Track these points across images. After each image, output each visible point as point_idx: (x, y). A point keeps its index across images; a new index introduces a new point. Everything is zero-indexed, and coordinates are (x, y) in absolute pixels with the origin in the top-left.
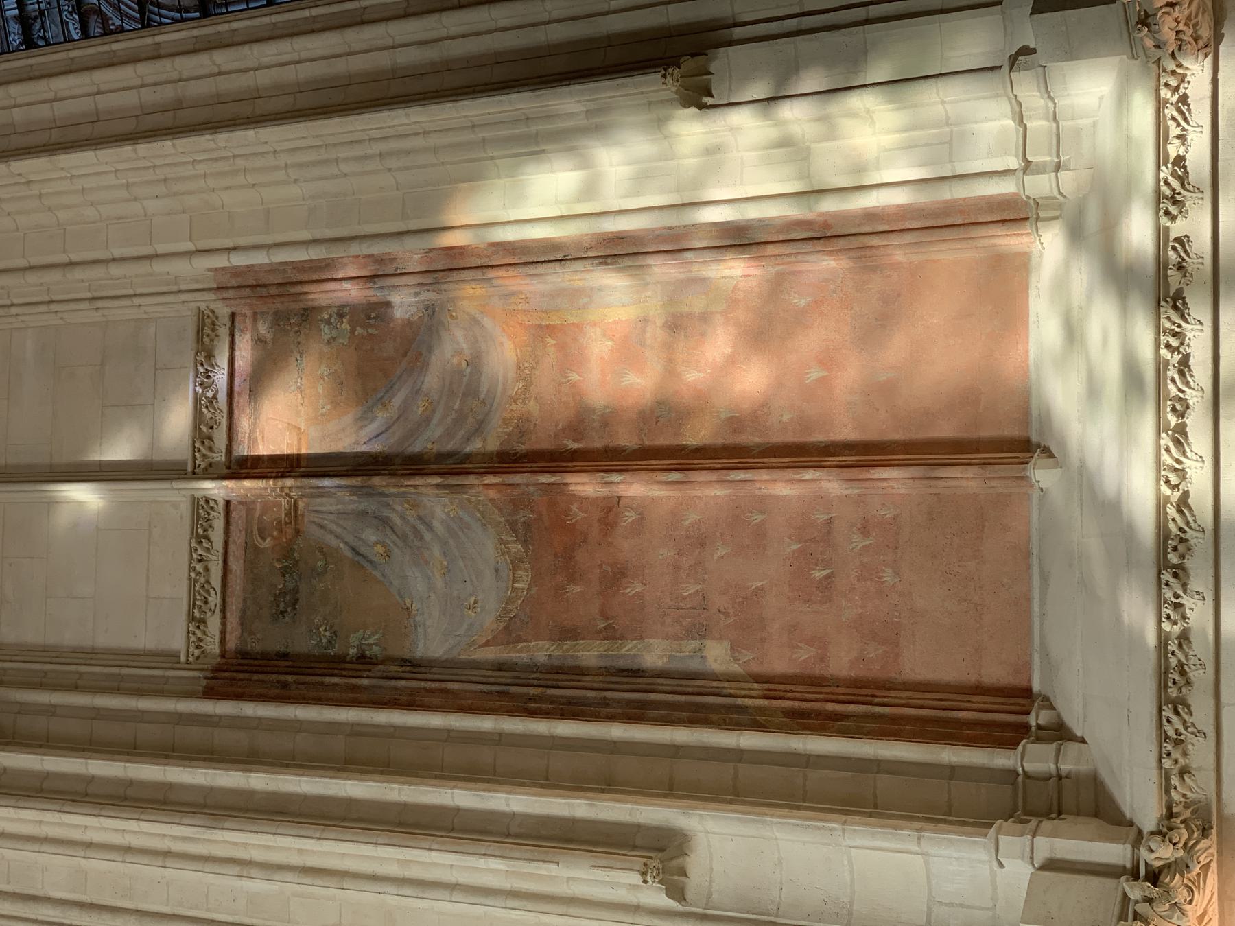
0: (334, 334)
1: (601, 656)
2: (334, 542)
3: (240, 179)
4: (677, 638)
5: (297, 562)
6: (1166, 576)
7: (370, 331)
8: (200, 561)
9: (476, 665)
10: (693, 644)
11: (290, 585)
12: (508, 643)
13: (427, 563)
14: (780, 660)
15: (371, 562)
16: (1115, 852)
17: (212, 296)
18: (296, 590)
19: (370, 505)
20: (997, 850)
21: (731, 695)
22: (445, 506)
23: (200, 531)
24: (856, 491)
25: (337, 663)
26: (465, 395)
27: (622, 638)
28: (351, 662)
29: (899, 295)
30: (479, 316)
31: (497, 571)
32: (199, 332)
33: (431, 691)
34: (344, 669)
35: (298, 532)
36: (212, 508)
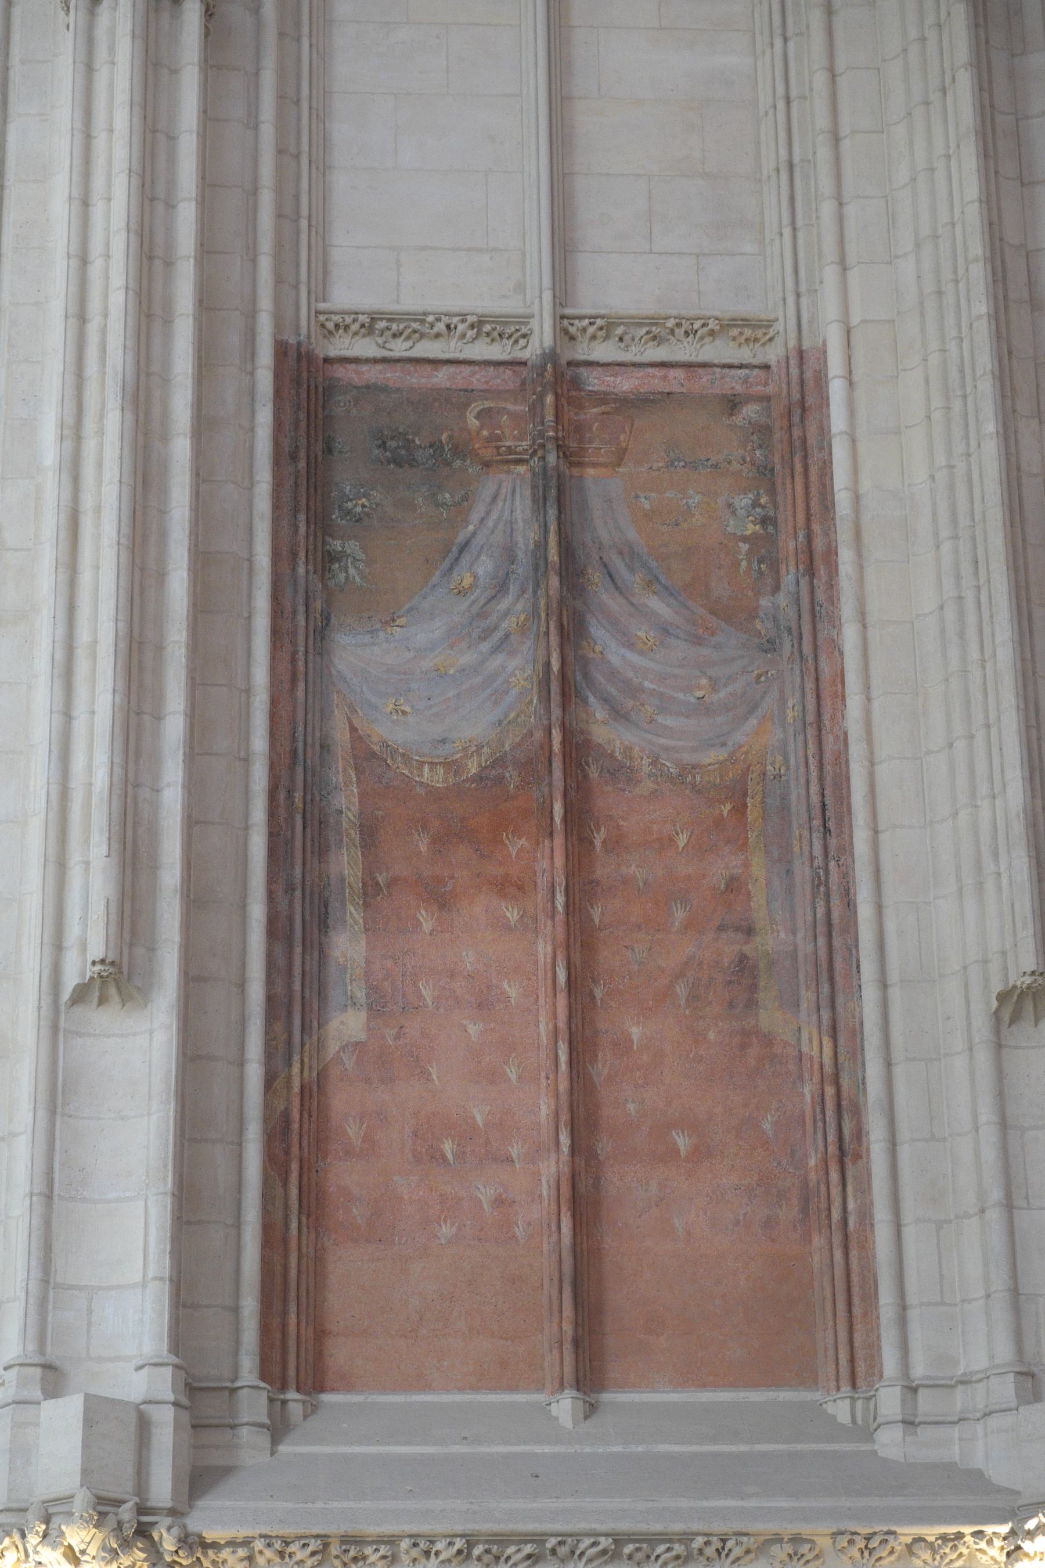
0: (741, 513)
1: (343, 880)
2: (475, 516)
3: (937, 402)
4: (368, 974)
5: (448, 464)
6: (459, 1543)
7: (744, 564)
8: (448, 327)
9: (325, 714)
10: (361, 995)
11: (419, 455)
12: (355, 757)
13: (451, 646)
14: (345, 1103)
15: (451, 569)
16: (162, 1488)
17: (792, 343)
18: (413, 463)
19: (522, 568)
20: (156, 1365)
21: (303, 1045)
22: (523, 670)
23: (487, 328)
24: (545, 1193)
25: (321, 525)
26: (661, 695)
27: (366, 905)
28: (324, 543)
29: (773, 1241)
30: (759, 712)
31: (443, 741)
32: (745, 322)
33: (293, 661)
34: (315, 536)
35: (487, 465)
36: (516, 342)
